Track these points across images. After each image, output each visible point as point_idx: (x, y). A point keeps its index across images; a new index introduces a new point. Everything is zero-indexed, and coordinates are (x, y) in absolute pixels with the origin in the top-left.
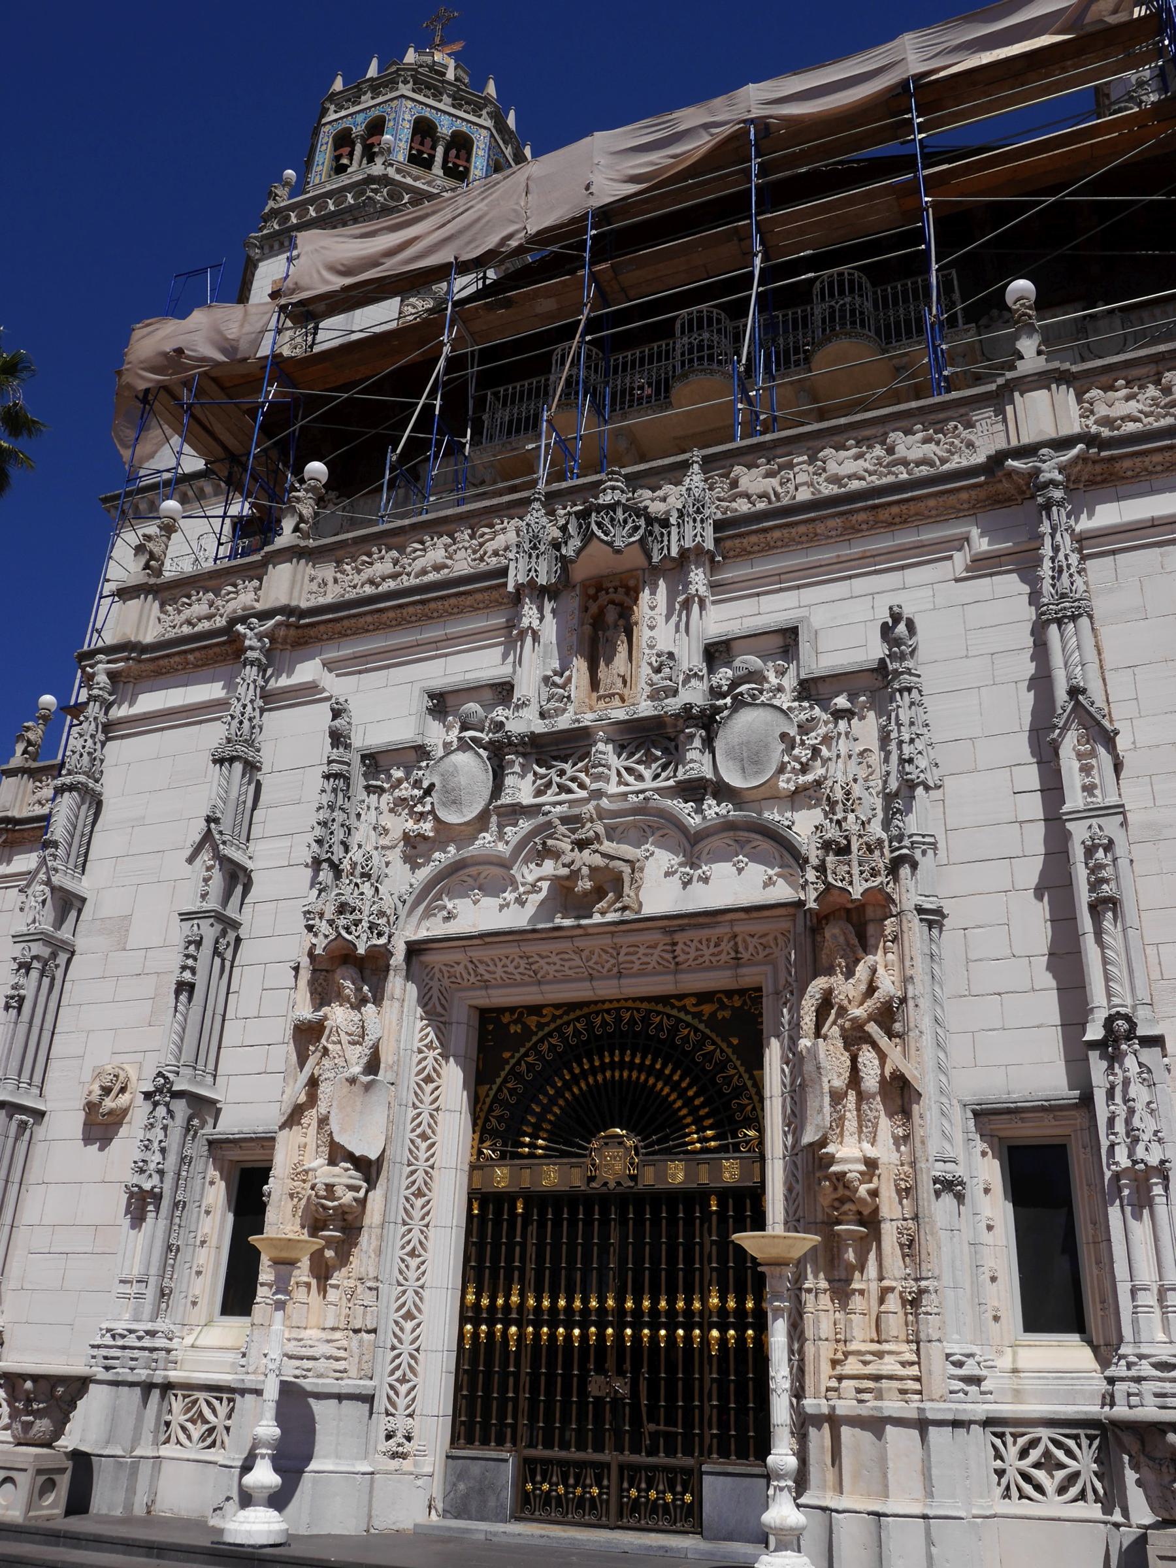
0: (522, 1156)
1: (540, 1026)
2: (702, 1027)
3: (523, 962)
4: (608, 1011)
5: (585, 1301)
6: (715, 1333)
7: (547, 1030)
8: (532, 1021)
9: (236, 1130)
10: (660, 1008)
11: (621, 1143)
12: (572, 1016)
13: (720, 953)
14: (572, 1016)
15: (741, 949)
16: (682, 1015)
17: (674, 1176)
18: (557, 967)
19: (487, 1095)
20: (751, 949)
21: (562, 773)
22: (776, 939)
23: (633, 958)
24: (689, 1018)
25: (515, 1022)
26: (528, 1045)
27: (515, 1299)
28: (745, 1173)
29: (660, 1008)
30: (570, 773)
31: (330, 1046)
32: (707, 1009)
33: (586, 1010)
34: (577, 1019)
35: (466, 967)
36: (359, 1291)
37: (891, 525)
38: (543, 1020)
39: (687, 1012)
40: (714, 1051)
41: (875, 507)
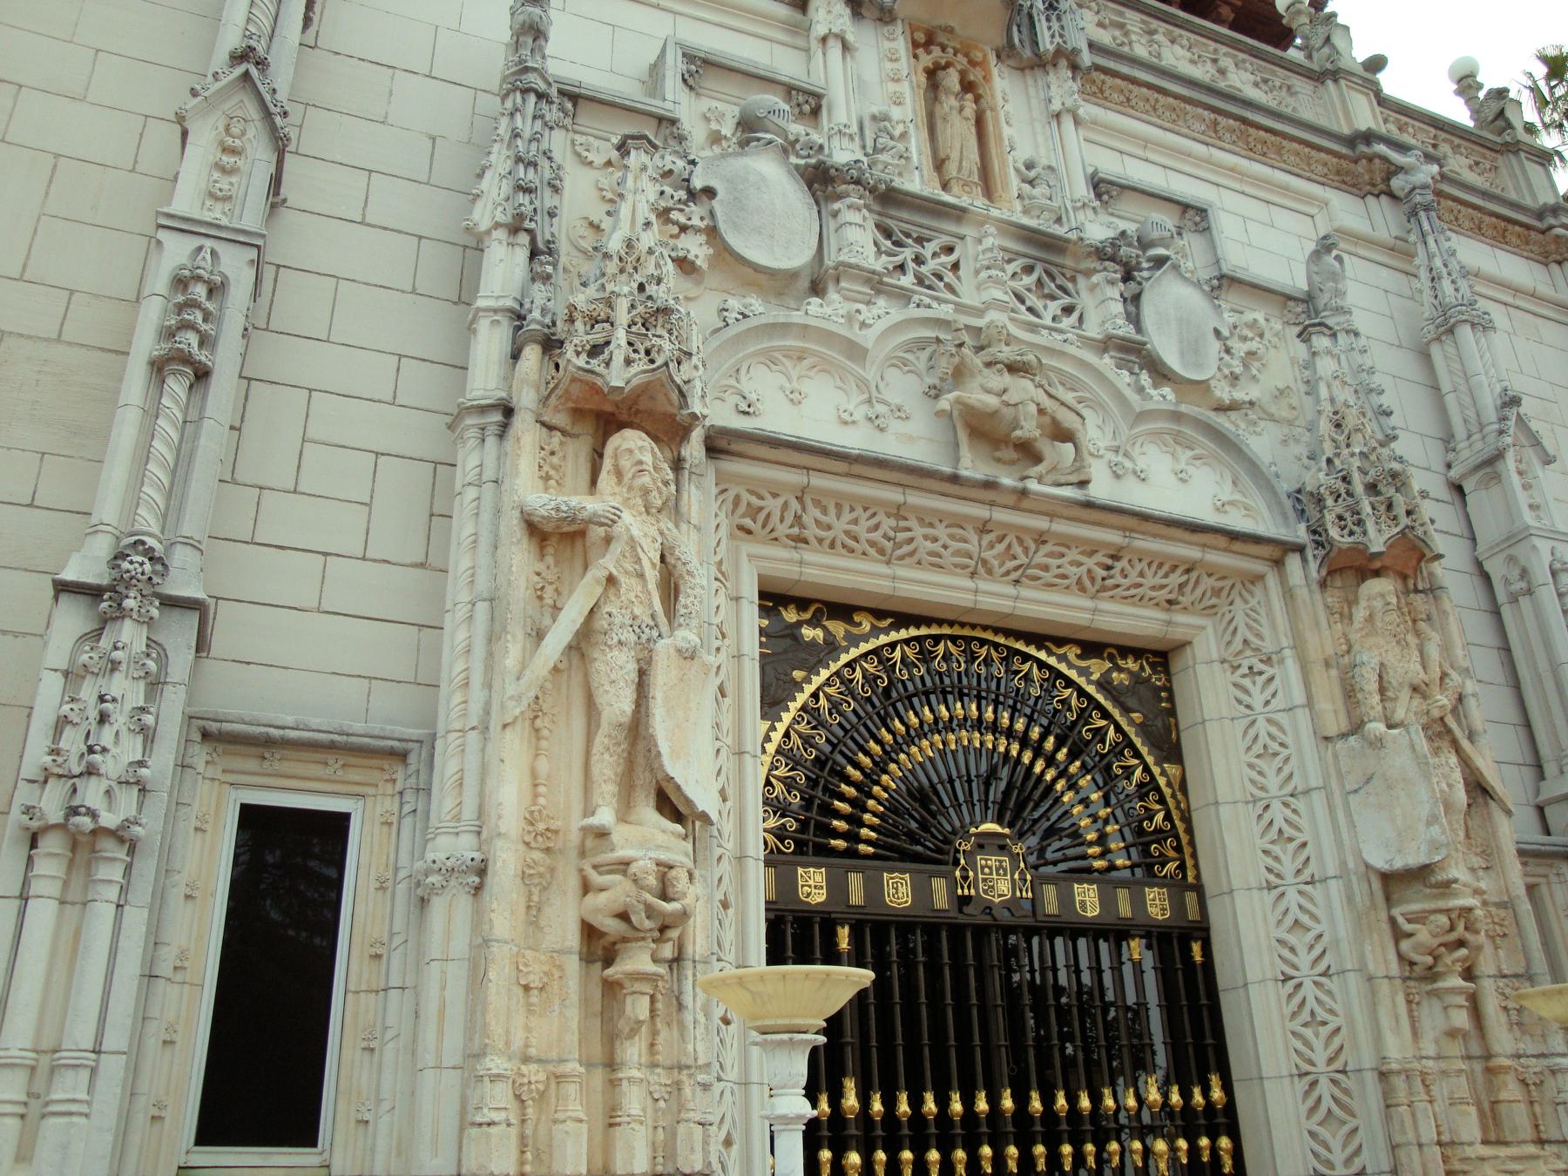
0: (833, 852)
1: (854, 641)
2: (1091, 689)
3: (888, 524)
4: (954, 639)
5: (916, 1102)
6: (1204, 1142)
7: (865, 647)
8: (838, 628)
9: (289, 720)
10: (1032, 650)
11: (1002, 848)
12: (904, 634)
13: (1163, 587)
14: (904, 634)
15: (1188, 589)
16: (1063, 667)
17: (1083, 903)
18: (936, 547)
19: (767, 739)
20: (1199, 592)
21: (919, 260)
22: (1233, 586)
23: (1053, 562)
24: (1072, 674)
25: (814, 622)
26: (834, 667)
27: (851, 1101)
28: (1178, 906)
29: (1032, 650)
30: (932, 265)
31: (622, 579)
32: (1098, 667)
33: (924, 631)
34: (907, 642)
35: (785, 505)
36: (687, 1091)
37: (1251, 152)
38: (855, 630)
39: (1070, 666)
40: (1106, 728)
41: (1244, 121)
